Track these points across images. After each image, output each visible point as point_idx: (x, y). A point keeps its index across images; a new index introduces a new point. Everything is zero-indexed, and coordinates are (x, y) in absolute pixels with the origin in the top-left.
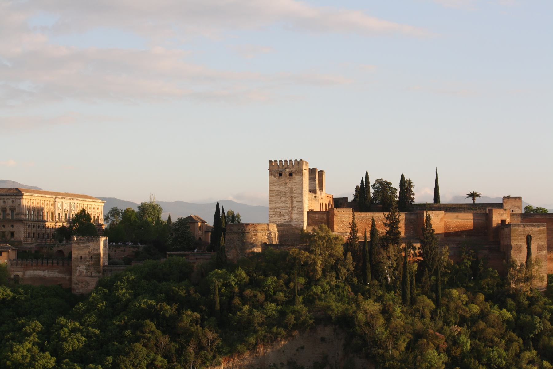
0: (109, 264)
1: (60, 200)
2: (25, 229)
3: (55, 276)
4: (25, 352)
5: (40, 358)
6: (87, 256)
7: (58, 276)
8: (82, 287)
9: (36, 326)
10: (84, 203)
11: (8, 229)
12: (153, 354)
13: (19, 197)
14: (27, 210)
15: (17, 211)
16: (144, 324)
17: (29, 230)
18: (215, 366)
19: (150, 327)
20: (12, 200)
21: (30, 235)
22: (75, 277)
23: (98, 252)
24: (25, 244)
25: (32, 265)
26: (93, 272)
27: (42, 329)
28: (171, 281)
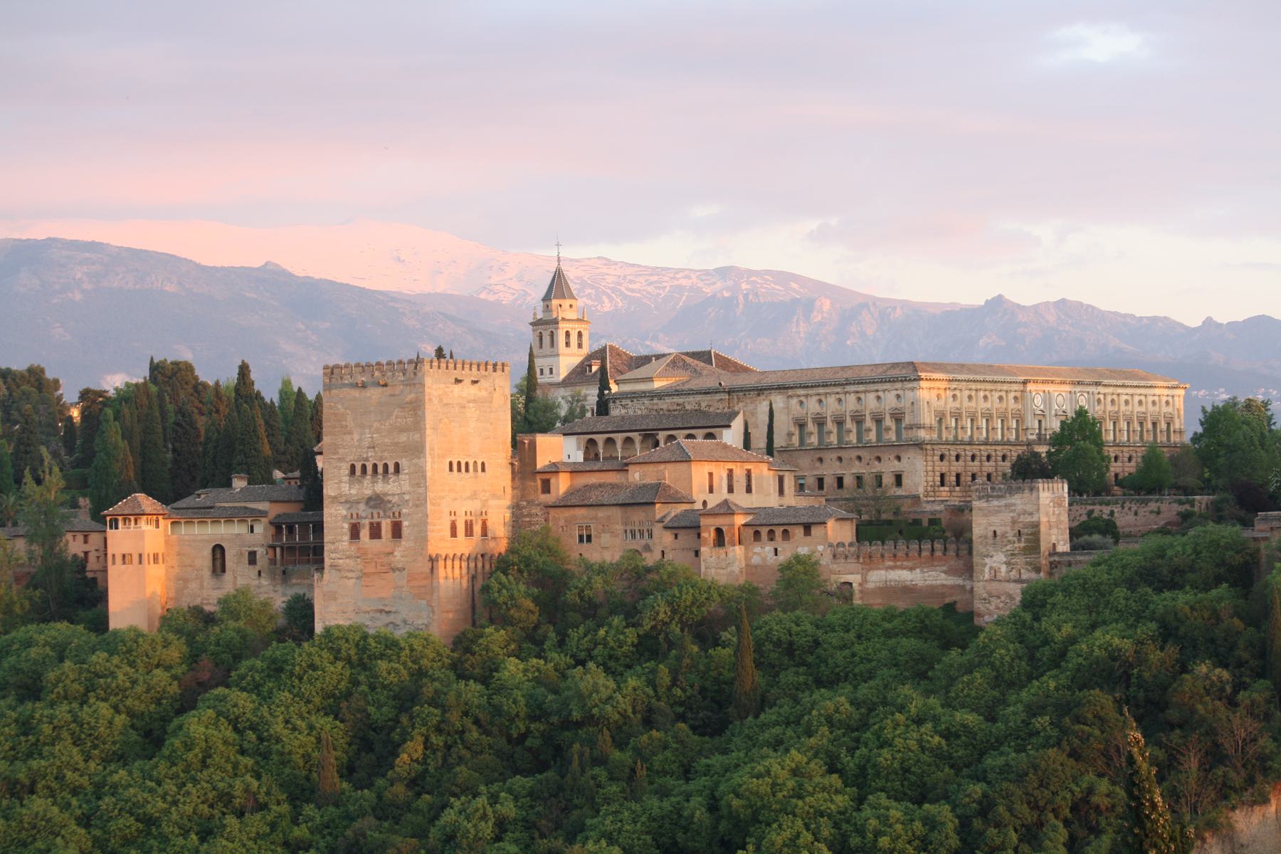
0: (1073, 548)
1: (1041, 387)
2: (930, 463)
3: (938, 582)
4: (783, 775)
5: (814, 789)
6: (1008, 529)
7: (945, 582)
8: (998, 608)
9: (837, 711)
10: (1120, 390)
11: (888, 467)
12: (1090, 777)
13: (910, 385)
14: (936, 416)
15: (907, 420)
16: (1084, 701)
17: (943, 467)
18: (1252, 806)
19: (1098, 708)
20: (895, 392)
21: (947, 479)
22: (981, 583)
23: (1035, 519)
24: (928, 502)
25: (882, 556)
26: (1022, 571)
27: (849, 717)
28: (1188, 588)
